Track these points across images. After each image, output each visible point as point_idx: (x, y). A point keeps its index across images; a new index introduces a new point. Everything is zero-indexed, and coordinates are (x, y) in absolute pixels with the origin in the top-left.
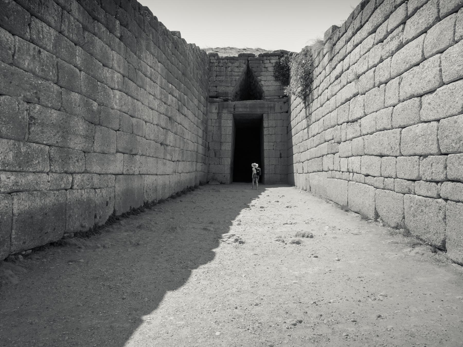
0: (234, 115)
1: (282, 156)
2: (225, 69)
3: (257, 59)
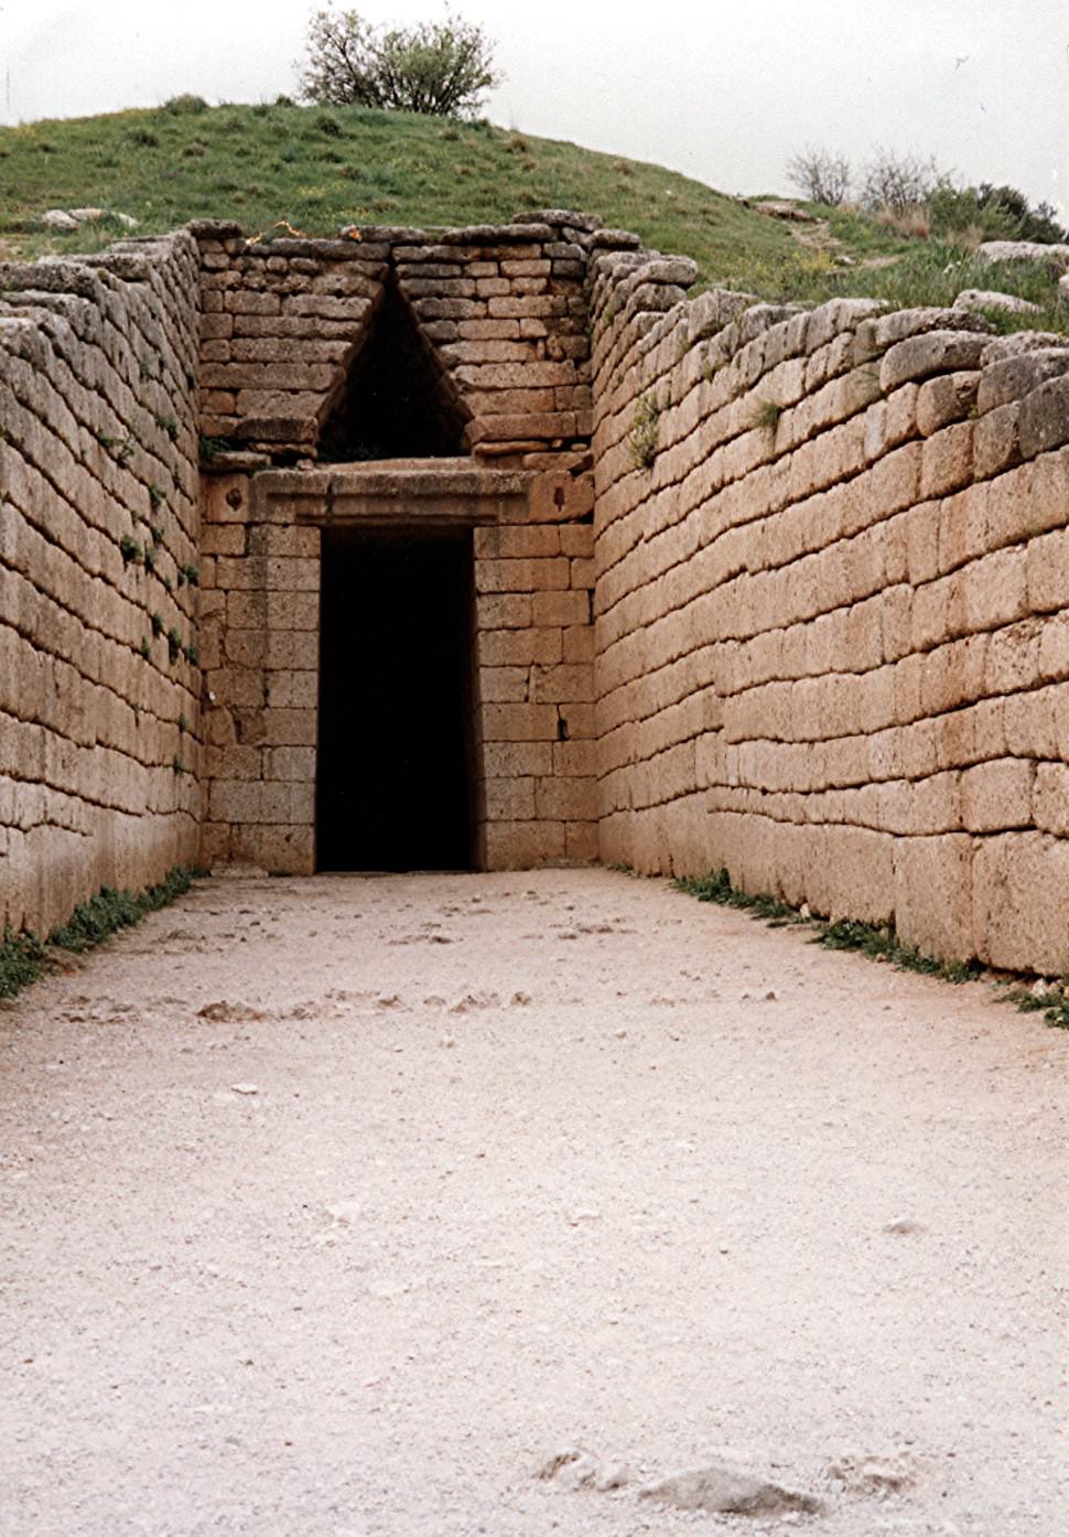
0: (324, 530)
1: (570, 731)
2: (276, 302)
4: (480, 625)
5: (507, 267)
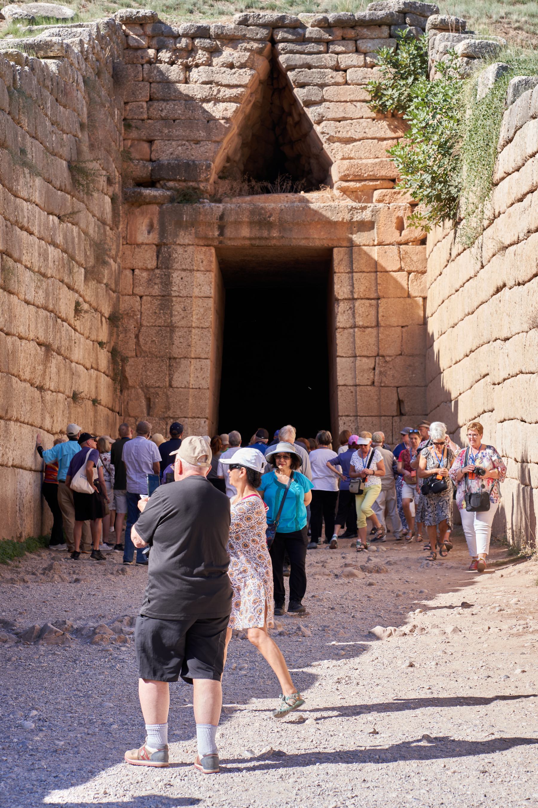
0: (217, 250)
1: (406, 408)
4: (338, 324)
5: (363, 45)
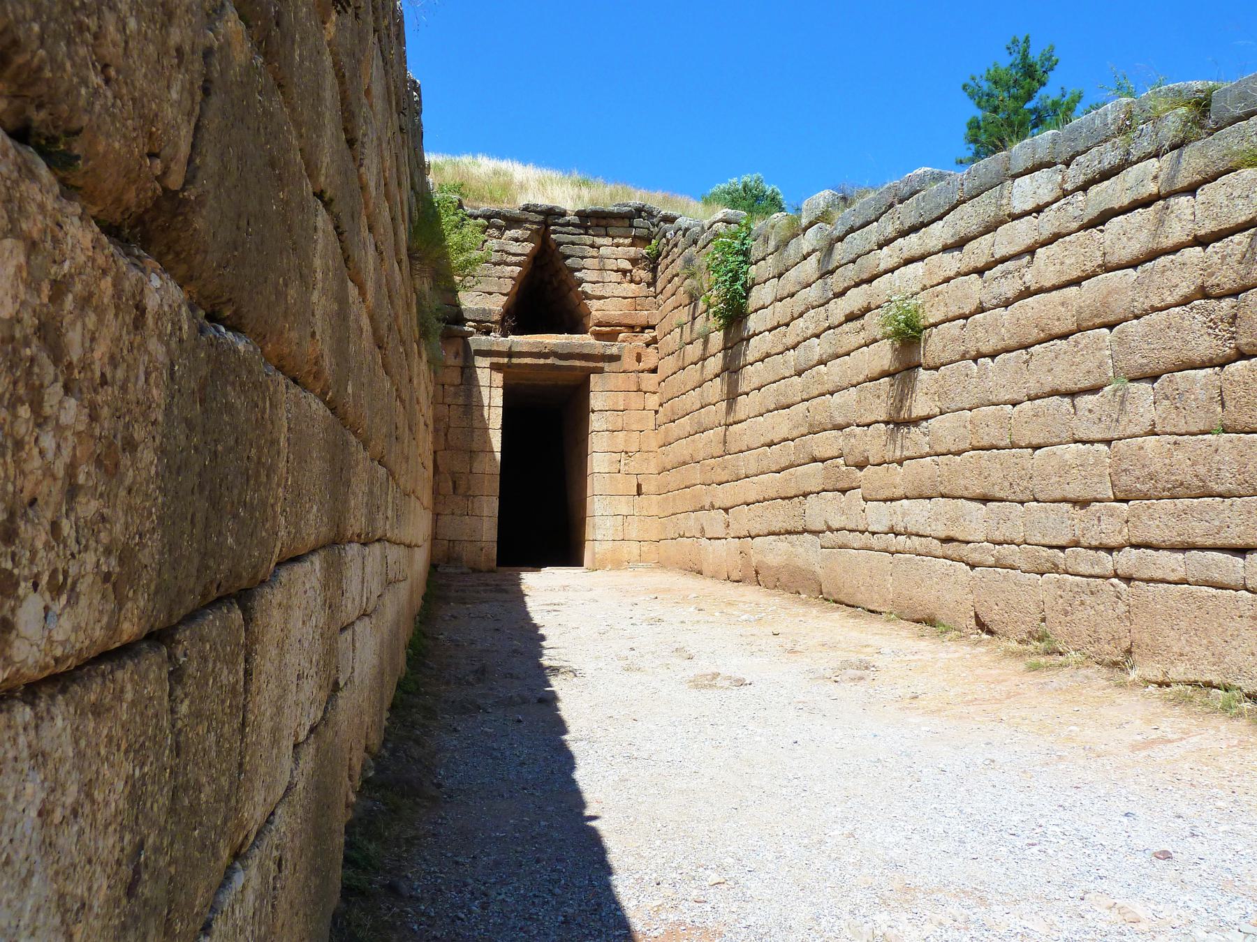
1: (644, 490)
3: (568, 224)
